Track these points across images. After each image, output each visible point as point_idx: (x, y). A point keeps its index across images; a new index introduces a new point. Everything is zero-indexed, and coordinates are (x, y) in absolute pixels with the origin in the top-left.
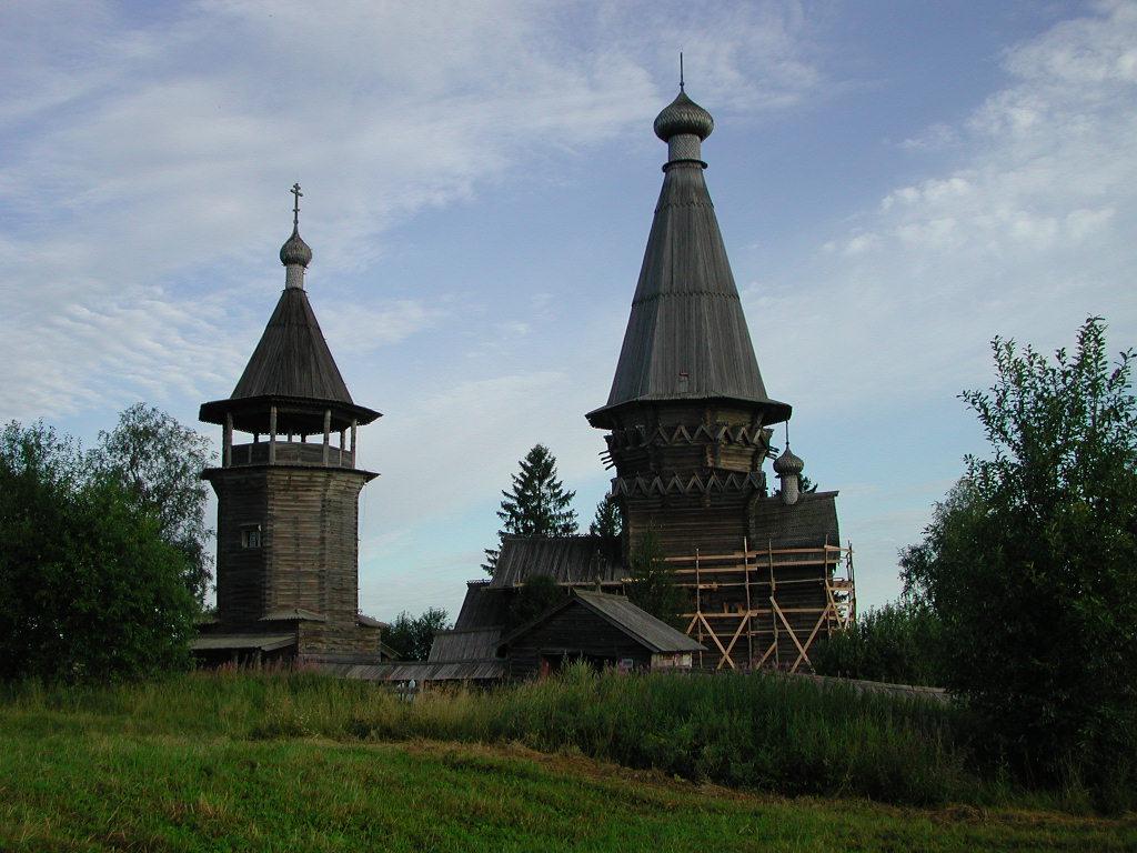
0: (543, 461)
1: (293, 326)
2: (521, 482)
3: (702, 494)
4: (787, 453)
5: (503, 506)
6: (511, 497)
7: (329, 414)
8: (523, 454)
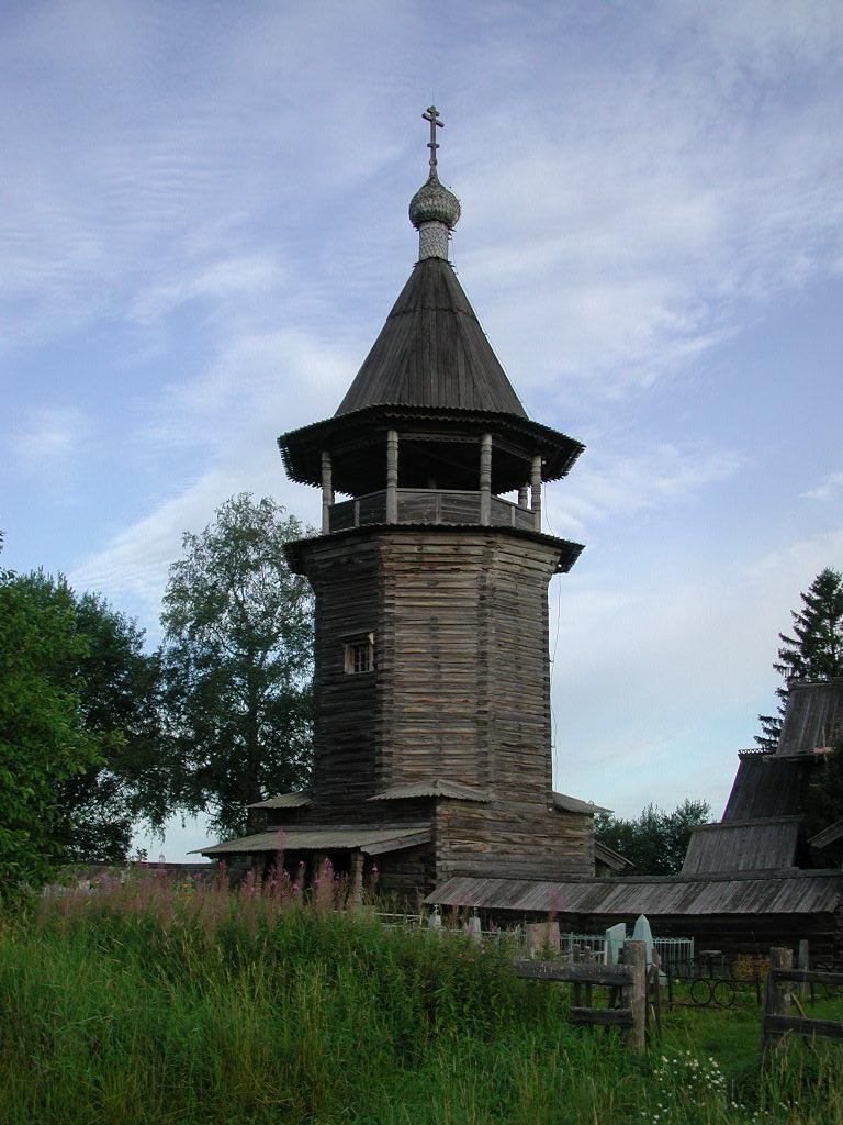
0: (835, 592)
1: (432, 313)
2: (805, 623)
5: (781, 656)
6: (793, 642)
7: (488, 441)
8: (806, 582)
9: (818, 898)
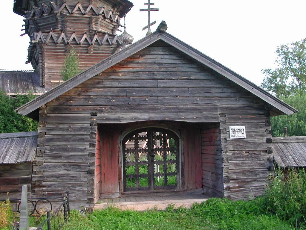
3: (89, 45)
4: (125, 33)
9: (20, 152)
